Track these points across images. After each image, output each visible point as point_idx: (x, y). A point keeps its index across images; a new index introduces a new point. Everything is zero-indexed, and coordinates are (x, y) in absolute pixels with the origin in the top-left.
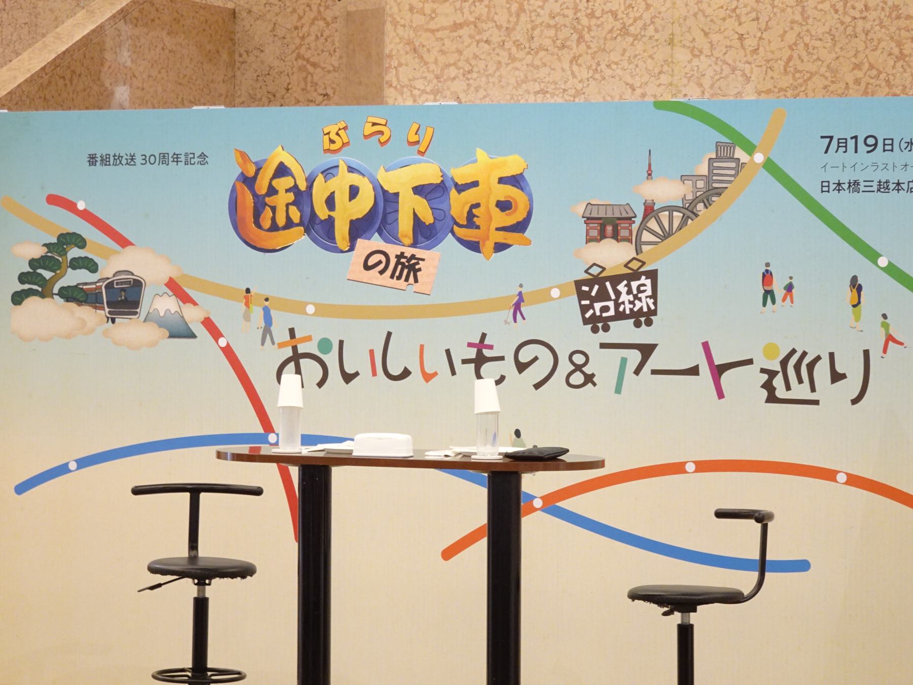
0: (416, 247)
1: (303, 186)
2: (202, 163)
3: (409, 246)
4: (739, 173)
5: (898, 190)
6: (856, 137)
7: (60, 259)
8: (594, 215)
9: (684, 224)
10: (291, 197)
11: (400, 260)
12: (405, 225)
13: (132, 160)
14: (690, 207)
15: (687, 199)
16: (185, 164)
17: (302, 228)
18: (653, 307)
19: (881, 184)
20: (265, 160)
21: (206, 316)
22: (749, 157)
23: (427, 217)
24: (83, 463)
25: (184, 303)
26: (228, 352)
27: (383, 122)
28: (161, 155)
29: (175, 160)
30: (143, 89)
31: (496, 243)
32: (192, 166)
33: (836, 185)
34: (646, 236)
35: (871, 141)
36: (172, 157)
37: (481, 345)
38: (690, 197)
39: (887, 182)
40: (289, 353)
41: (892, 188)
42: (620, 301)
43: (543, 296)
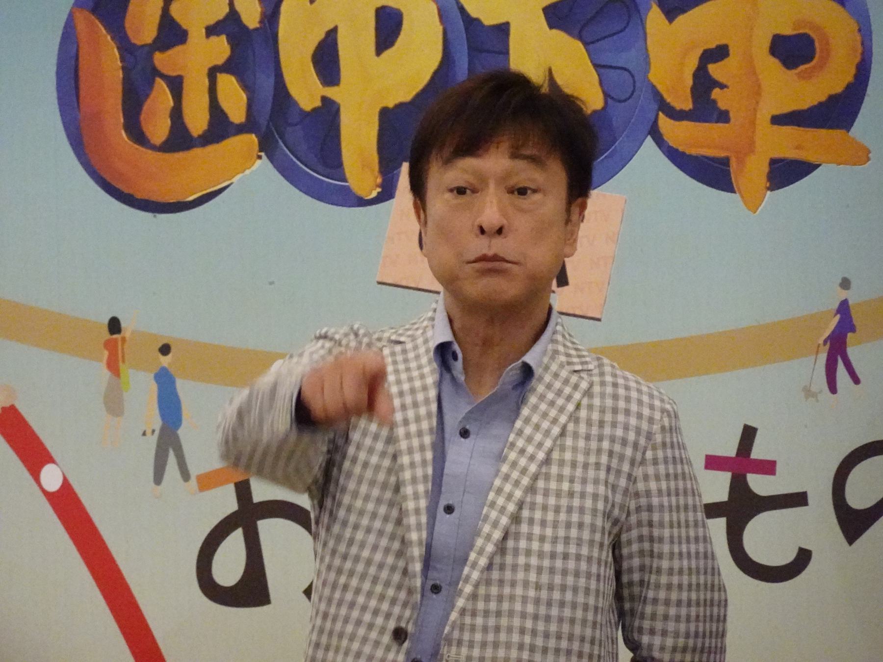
17: (253, 138)
31: (773, 162)
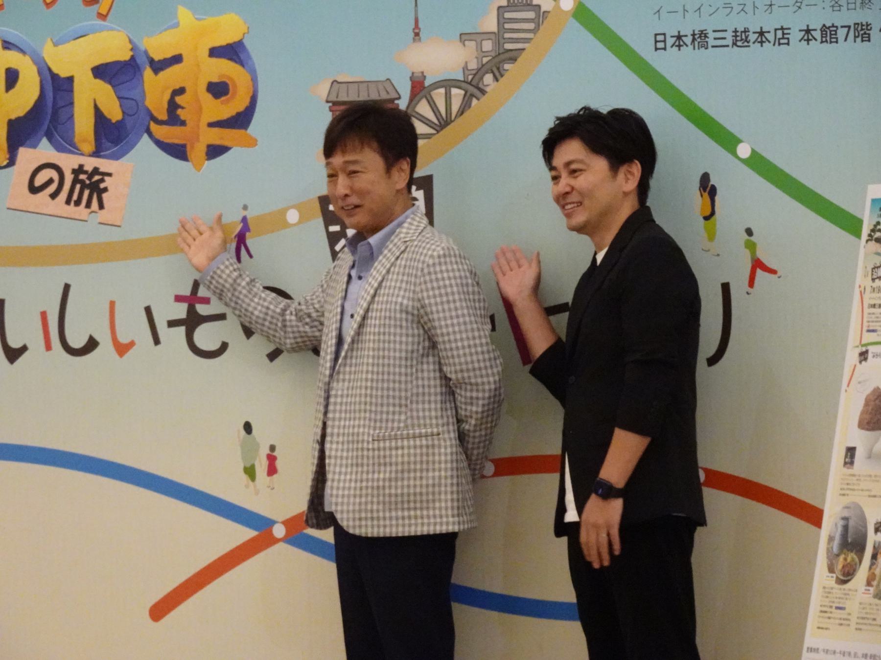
3: (90, 156)
4: (541, 28)
5: (762, 42)
9: (466, 108)
15: (469, 68)
19: (738, 34)
23: (114, 112)
31: (209, 146)
38: (473, 65)
39: (745, 32)
41: (752, 41)
43: (277, 221)
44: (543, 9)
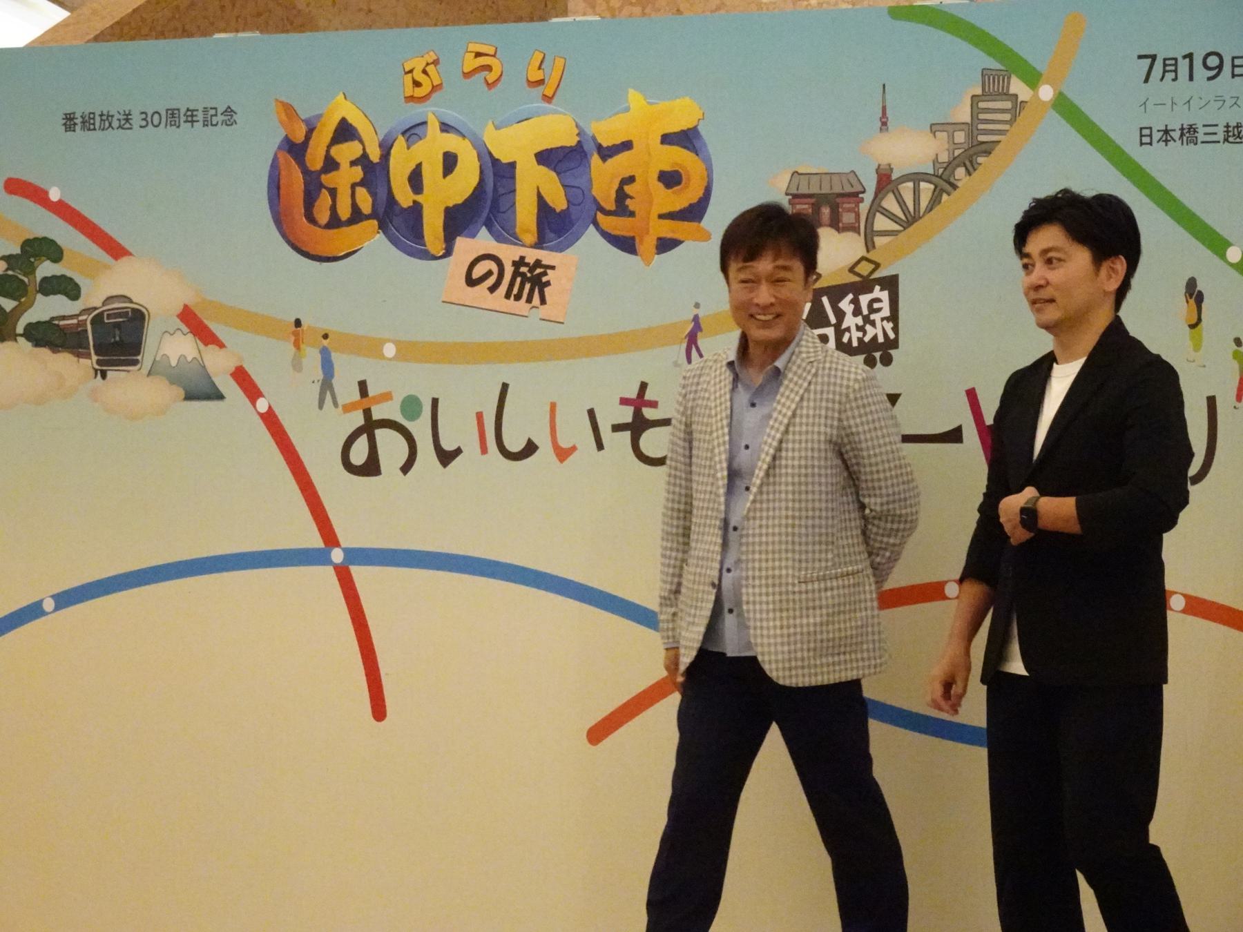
0: (542, 248)
1: (375, 155)
2: (228, 123)
3: (531, 247)
4: (1017, 118)
6: (1190, 56)
7: (26, 280)
8: (804, 190)
9: (937, 201)
10: (358, 173)
11: (520, 268)
12: (525, 214)
13: (127, 120)
14: (945, 173)
16: (204, 125)
18: (892, 335)
19: (1230, 129)
20: (319, 116)
21: (238, 364)
22: (1031, 92)
23: (558, 201)
24: (65, 599)
25: (206, 344)
26: (271, 420)
27: (491, 51)
28: (169, 112)
29: (190, 119)
30: (370, 11)
31: (659, 239)
32: (214, 127)
33: (1163, 133)
34: (881, 223)
35: (1213, 61)
36: (185, 115)
37: (639, 401)
38: (944, 158)
39: (1238, 127)
40: (358, 420)
42: (844, 326)
44: (1020, 99)
